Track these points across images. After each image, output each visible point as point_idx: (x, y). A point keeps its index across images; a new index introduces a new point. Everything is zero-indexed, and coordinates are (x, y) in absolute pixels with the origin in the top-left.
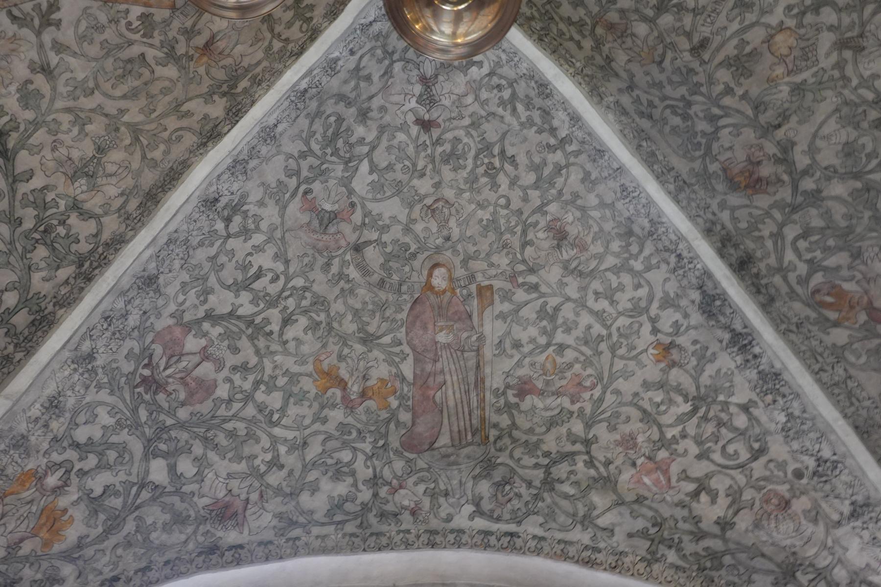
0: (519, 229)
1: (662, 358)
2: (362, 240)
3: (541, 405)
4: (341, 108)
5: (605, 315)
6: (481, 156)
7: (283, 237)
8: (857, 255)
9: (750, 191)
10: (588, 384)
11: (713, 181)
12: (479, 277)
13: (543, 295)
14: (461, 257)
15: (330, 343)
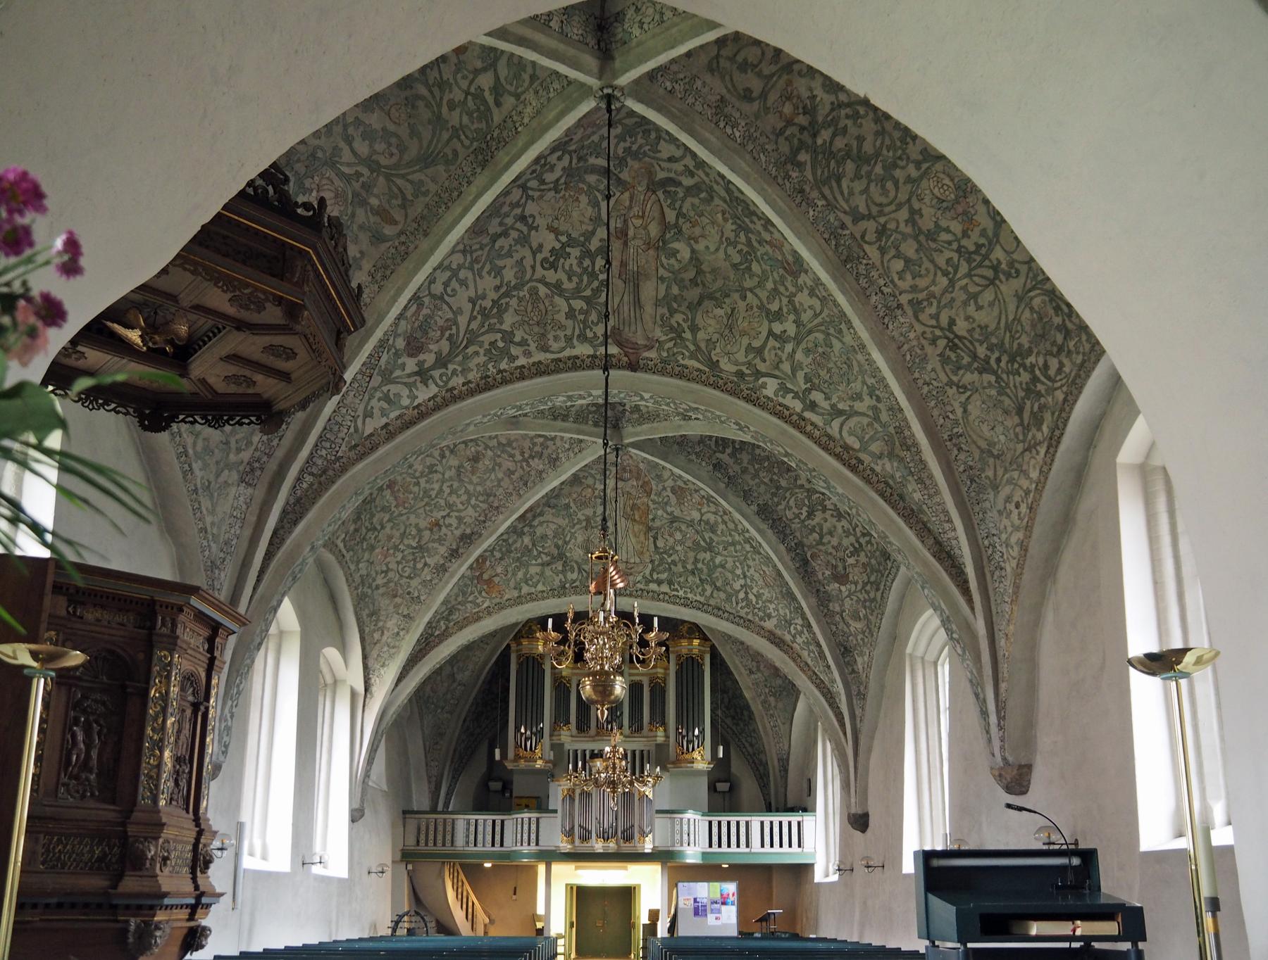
8: (501, 559)
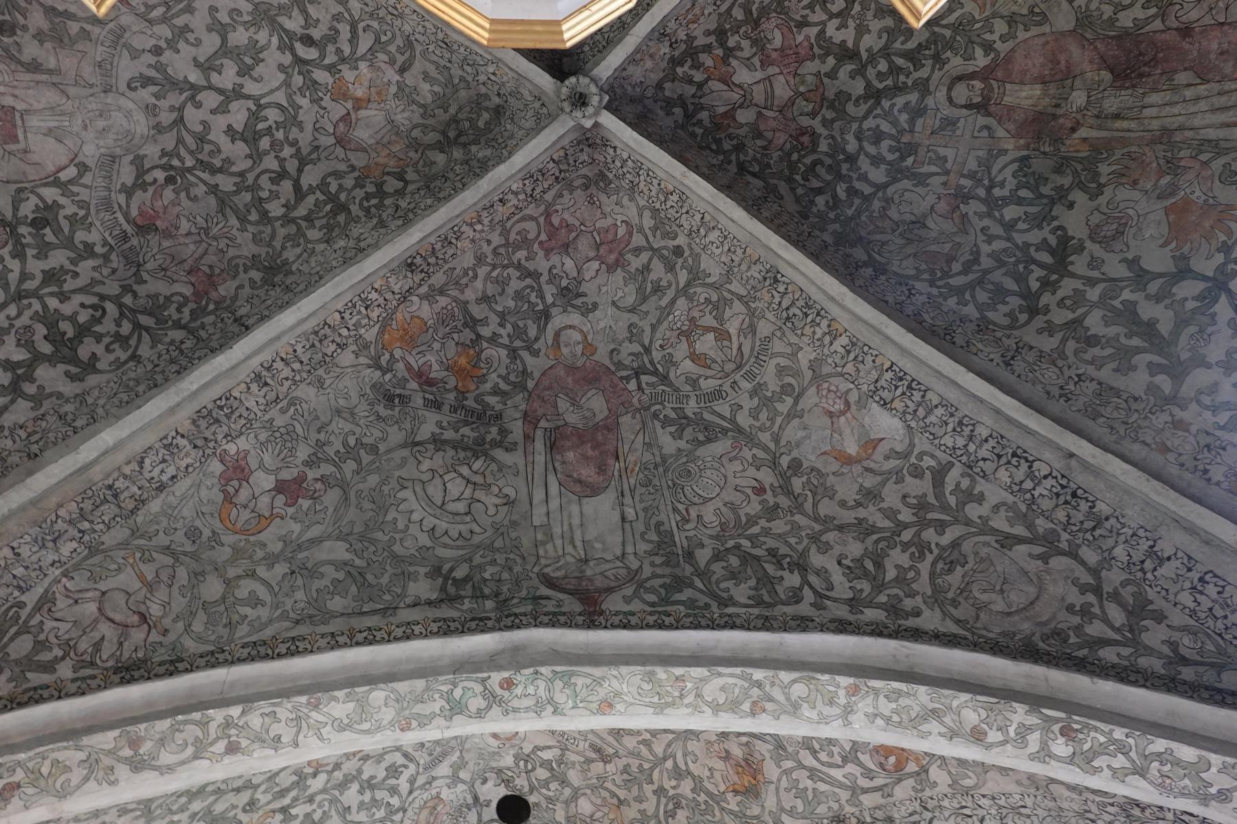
9: (759, 777)
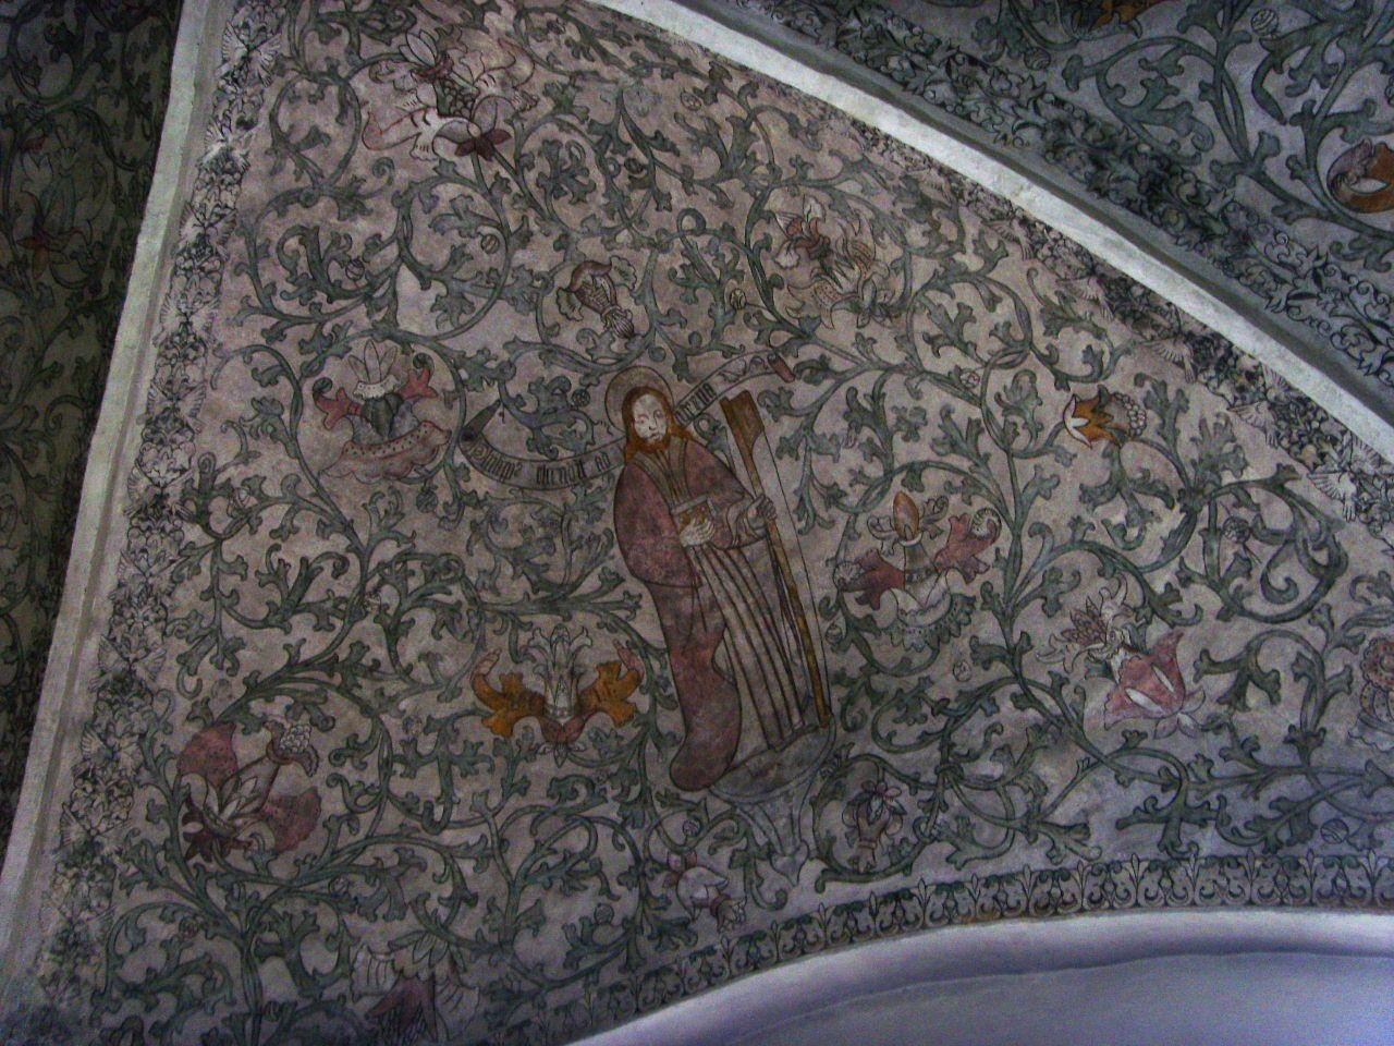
0: (743, 264)
1: (1097, 431)
2: (472, 414)
3: (913, 605)
4: (297, 215)
5: (963, 377)
6: (608, 154)
7: (319, 492)
10: (983, 531)
11: (1040, 26)
12: (719, 386)
13: (841, 378)
14: (671, 359)
15: (489, 634)
